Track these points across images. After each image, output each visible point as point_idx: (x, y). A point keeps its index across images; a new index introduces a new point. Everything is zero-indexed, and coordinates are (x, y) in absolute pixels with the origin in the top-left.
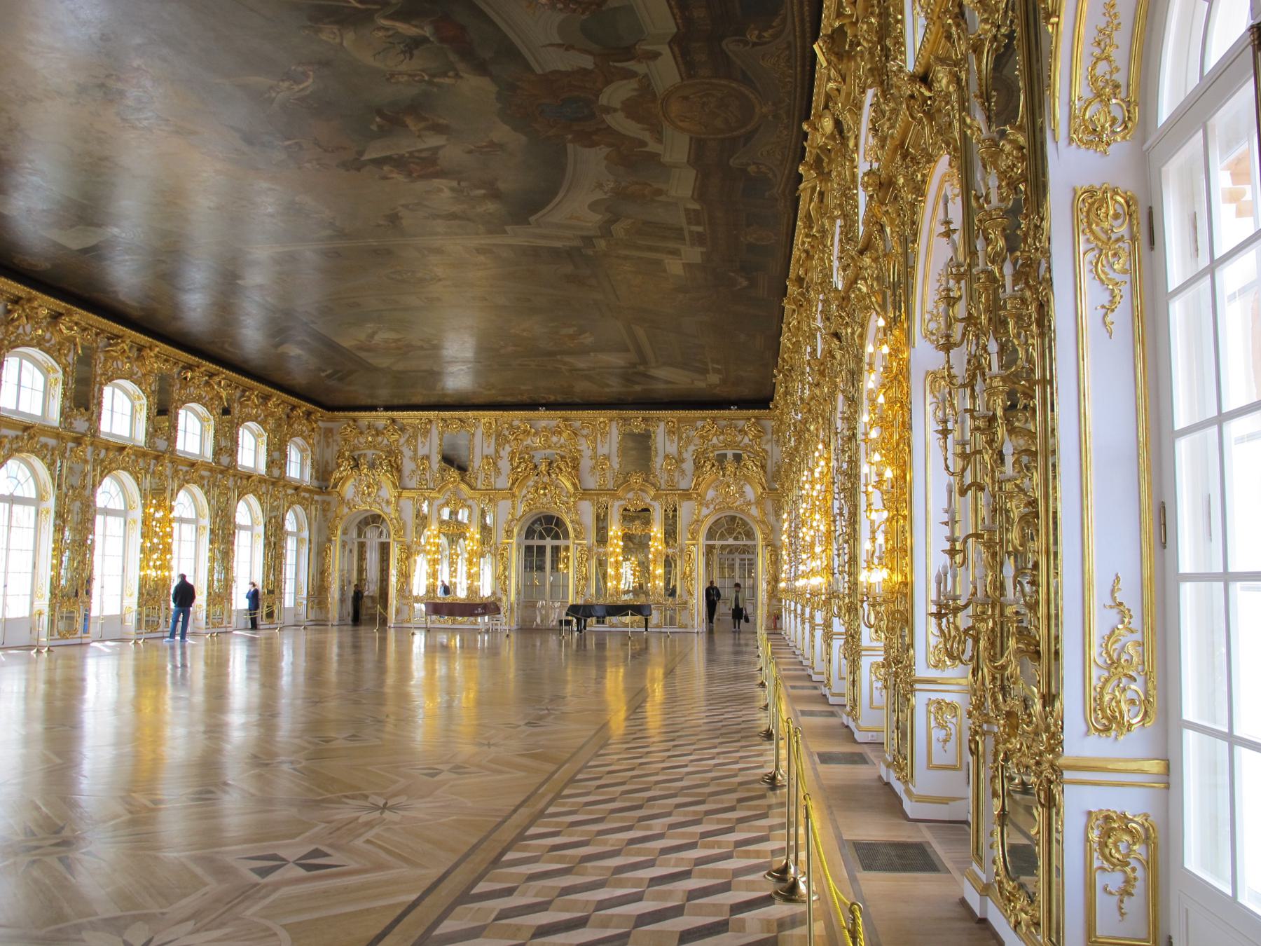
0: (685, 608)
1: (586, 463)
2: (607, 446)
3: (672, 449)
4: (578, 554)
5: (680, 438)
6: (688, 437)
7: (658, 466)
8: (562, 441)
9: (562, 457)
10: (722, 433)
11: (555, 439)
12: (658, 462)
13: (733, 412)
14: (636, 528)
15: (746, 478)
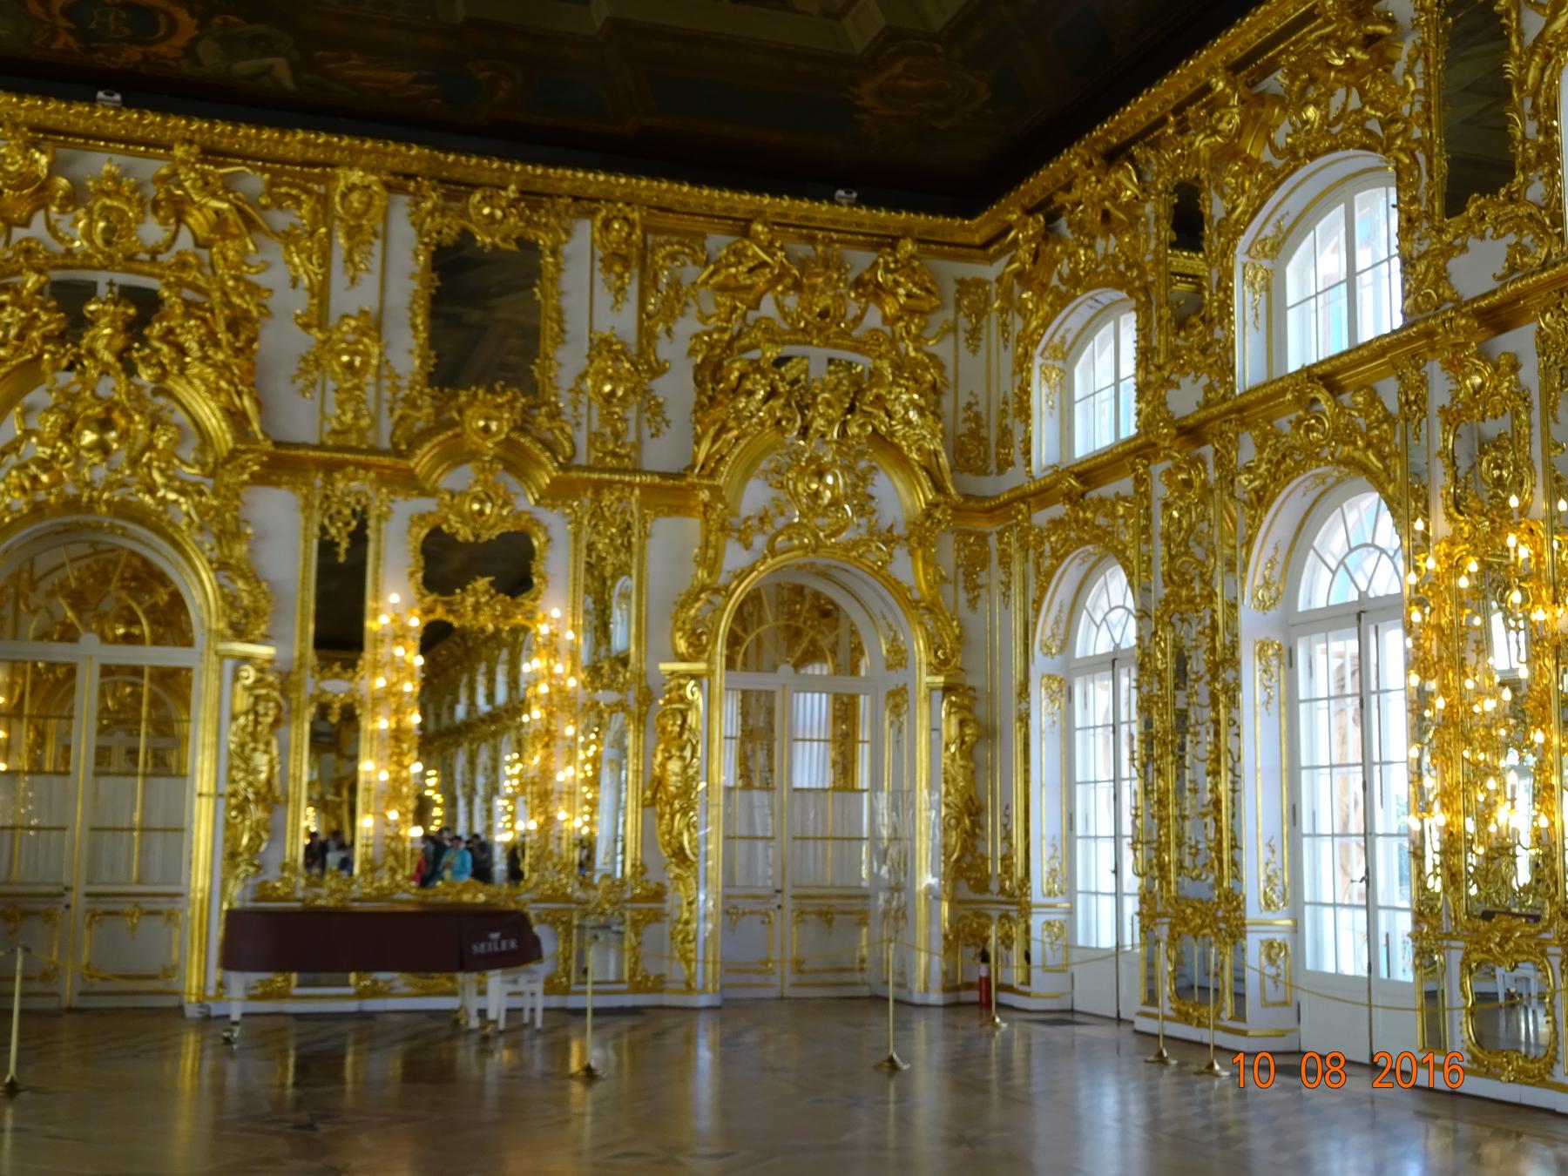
0: (658, 917)
1: (283, 340)
2: (370, 283)
3: (622, 322)
4: (242, 702)
5: (648, 284)
6: (675, 284)
7: (566, 379)
8: (185, 241)
9: (188, 304)
10: (797, 286)
11: (153, 231)
12: (566, 363)
13: (842, 210)
14: (478, 606)
15: (883, 442)
